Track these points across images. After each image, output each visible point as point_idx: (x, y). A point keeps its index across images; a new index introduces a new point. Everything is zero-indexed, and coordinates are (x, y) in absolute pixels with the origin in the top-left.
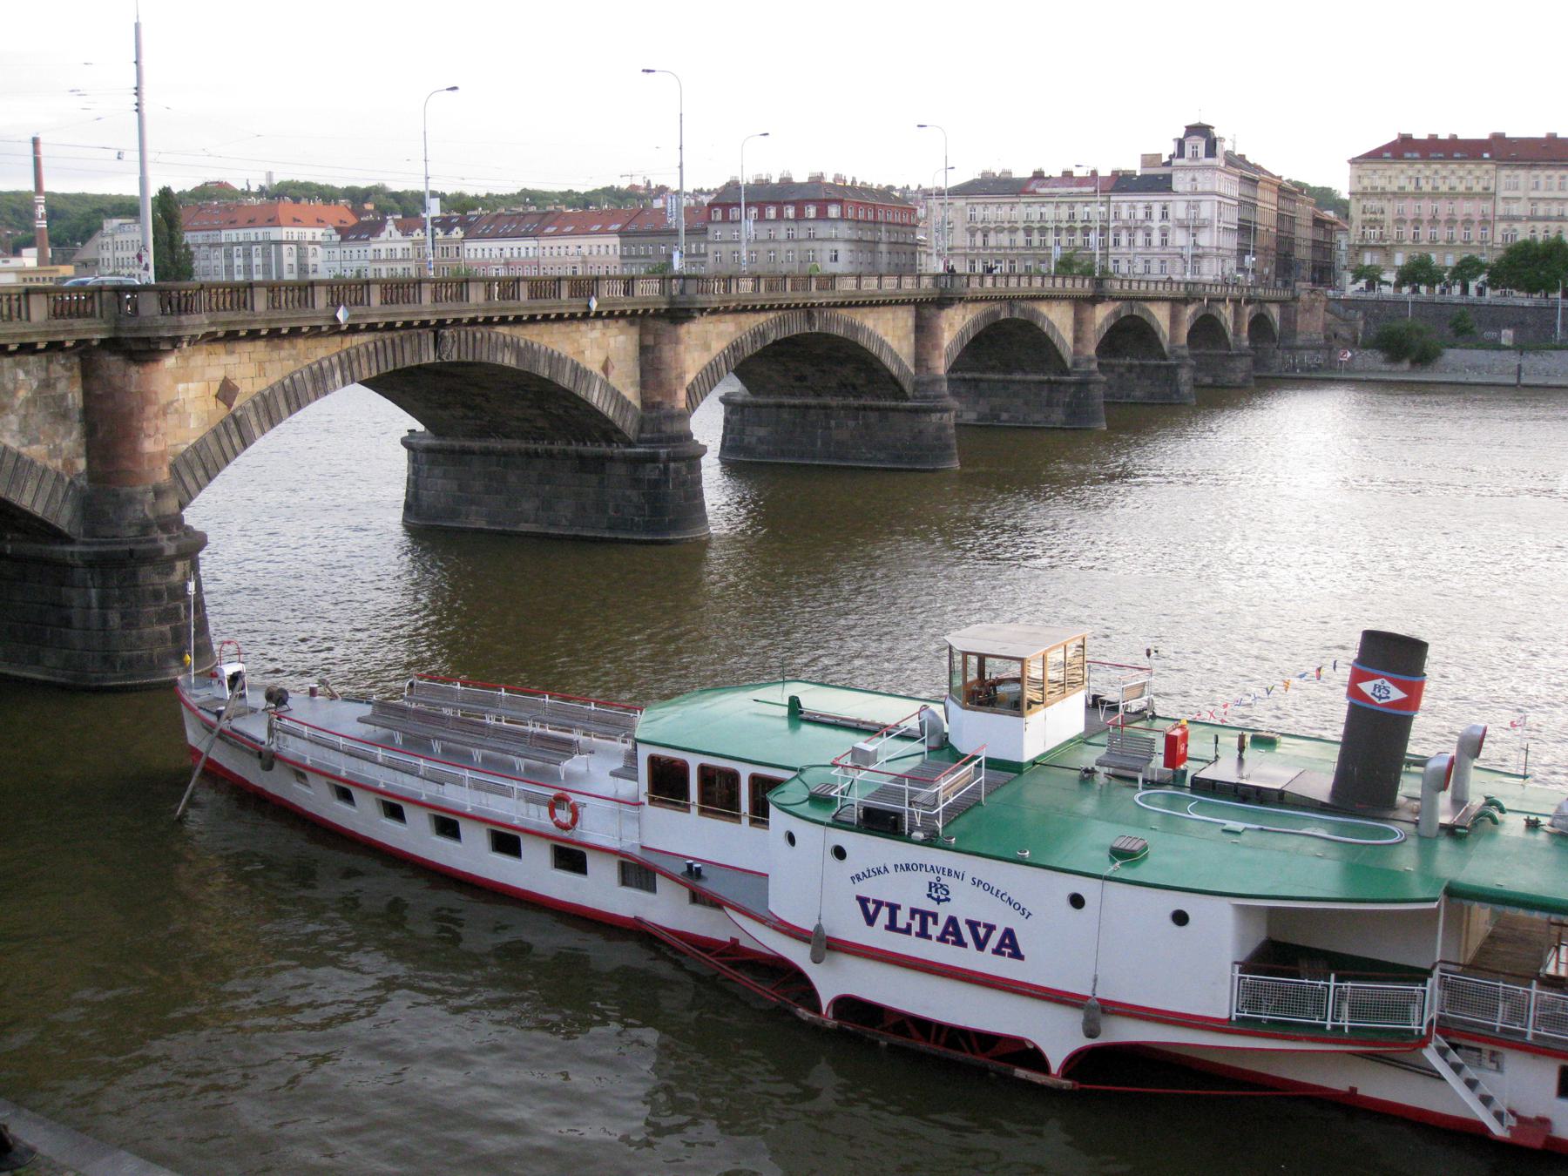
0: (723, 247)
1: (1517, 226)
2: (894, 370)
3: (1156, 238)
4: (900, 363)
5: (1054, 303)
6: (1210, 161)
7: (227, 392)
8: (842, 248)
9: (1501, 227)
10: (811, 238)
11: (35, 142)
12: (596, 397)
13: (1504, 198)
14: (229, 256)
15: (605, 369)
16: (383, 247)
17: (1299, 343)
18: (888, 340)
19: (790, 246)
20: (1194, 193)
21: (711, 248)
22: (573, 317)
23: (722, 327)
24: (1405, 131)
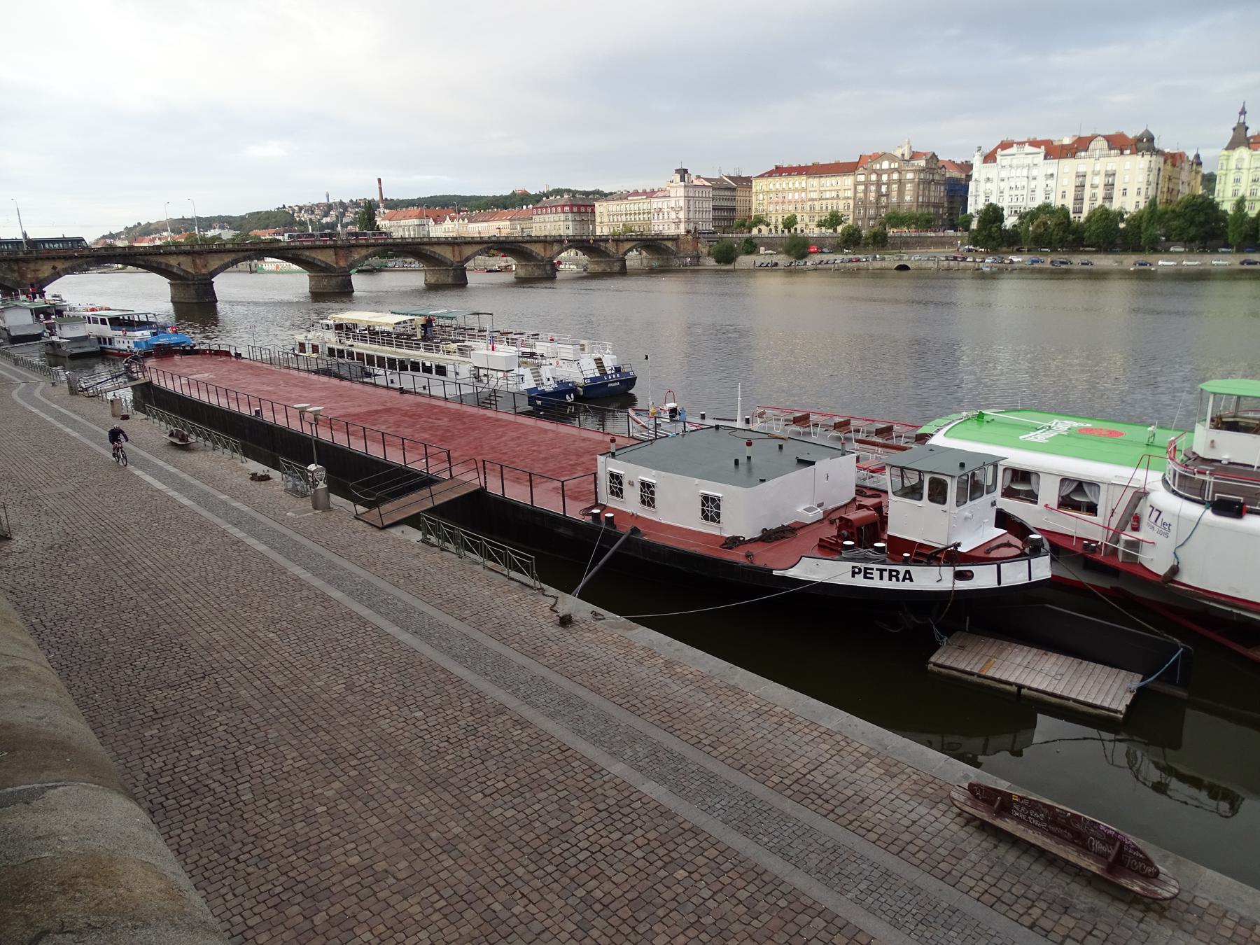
0: (538, 225)
1: (815, 203)
2: (323, 265)
3: (666, 217)
4: (326, 264)
5: (435, 246)
6: (682, 183)
7: (54, 268)
8: (570, 224)
9: (810, 203)
10: (544, 222)
11: (379, 180)
12: (175, 271)
13: (810, 191)
14: (404, 230)
15: (179, 264)
16: (446, 227)
17: (682, 255)
18: (320, 258)
19: (555, 224)
20: (676, 197)
21: (534, 225)
22: (156, 254)
23: (228, 255)
24: (779, 164)
